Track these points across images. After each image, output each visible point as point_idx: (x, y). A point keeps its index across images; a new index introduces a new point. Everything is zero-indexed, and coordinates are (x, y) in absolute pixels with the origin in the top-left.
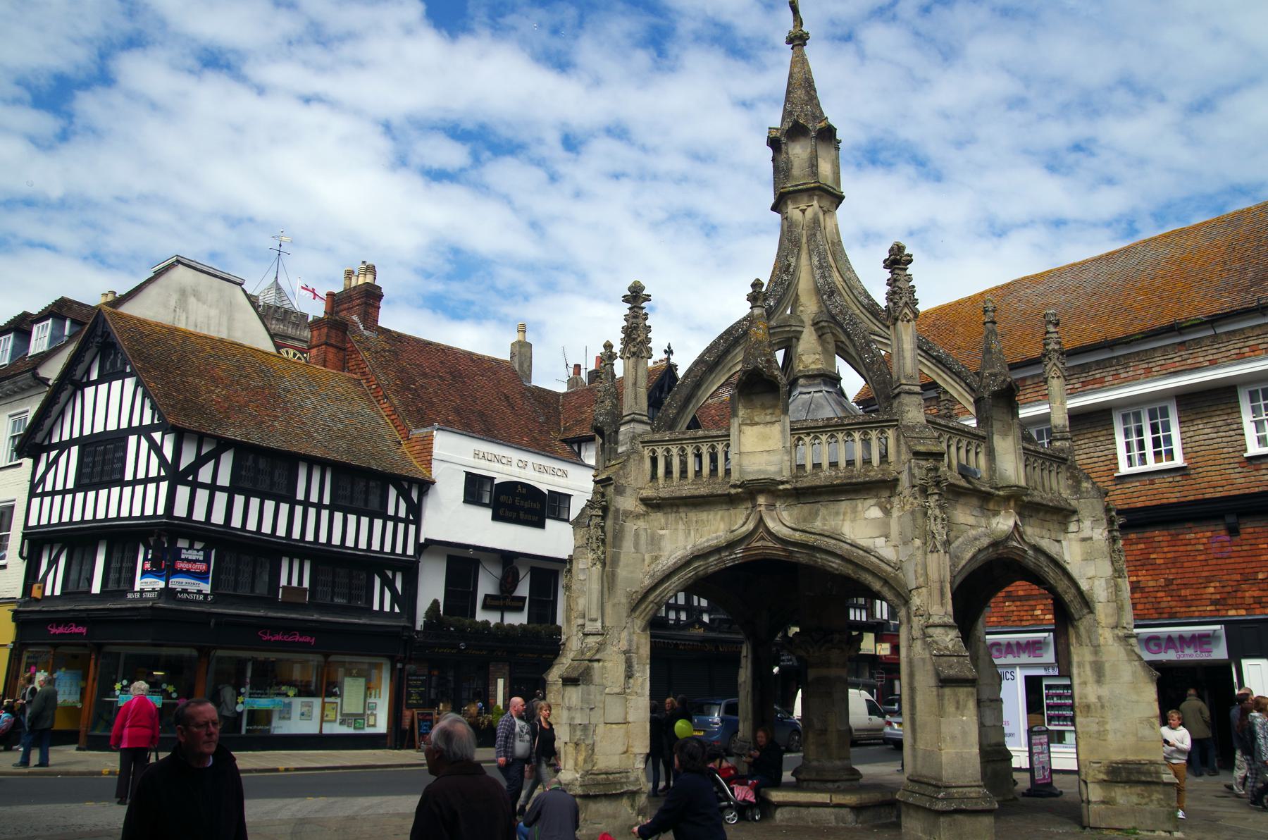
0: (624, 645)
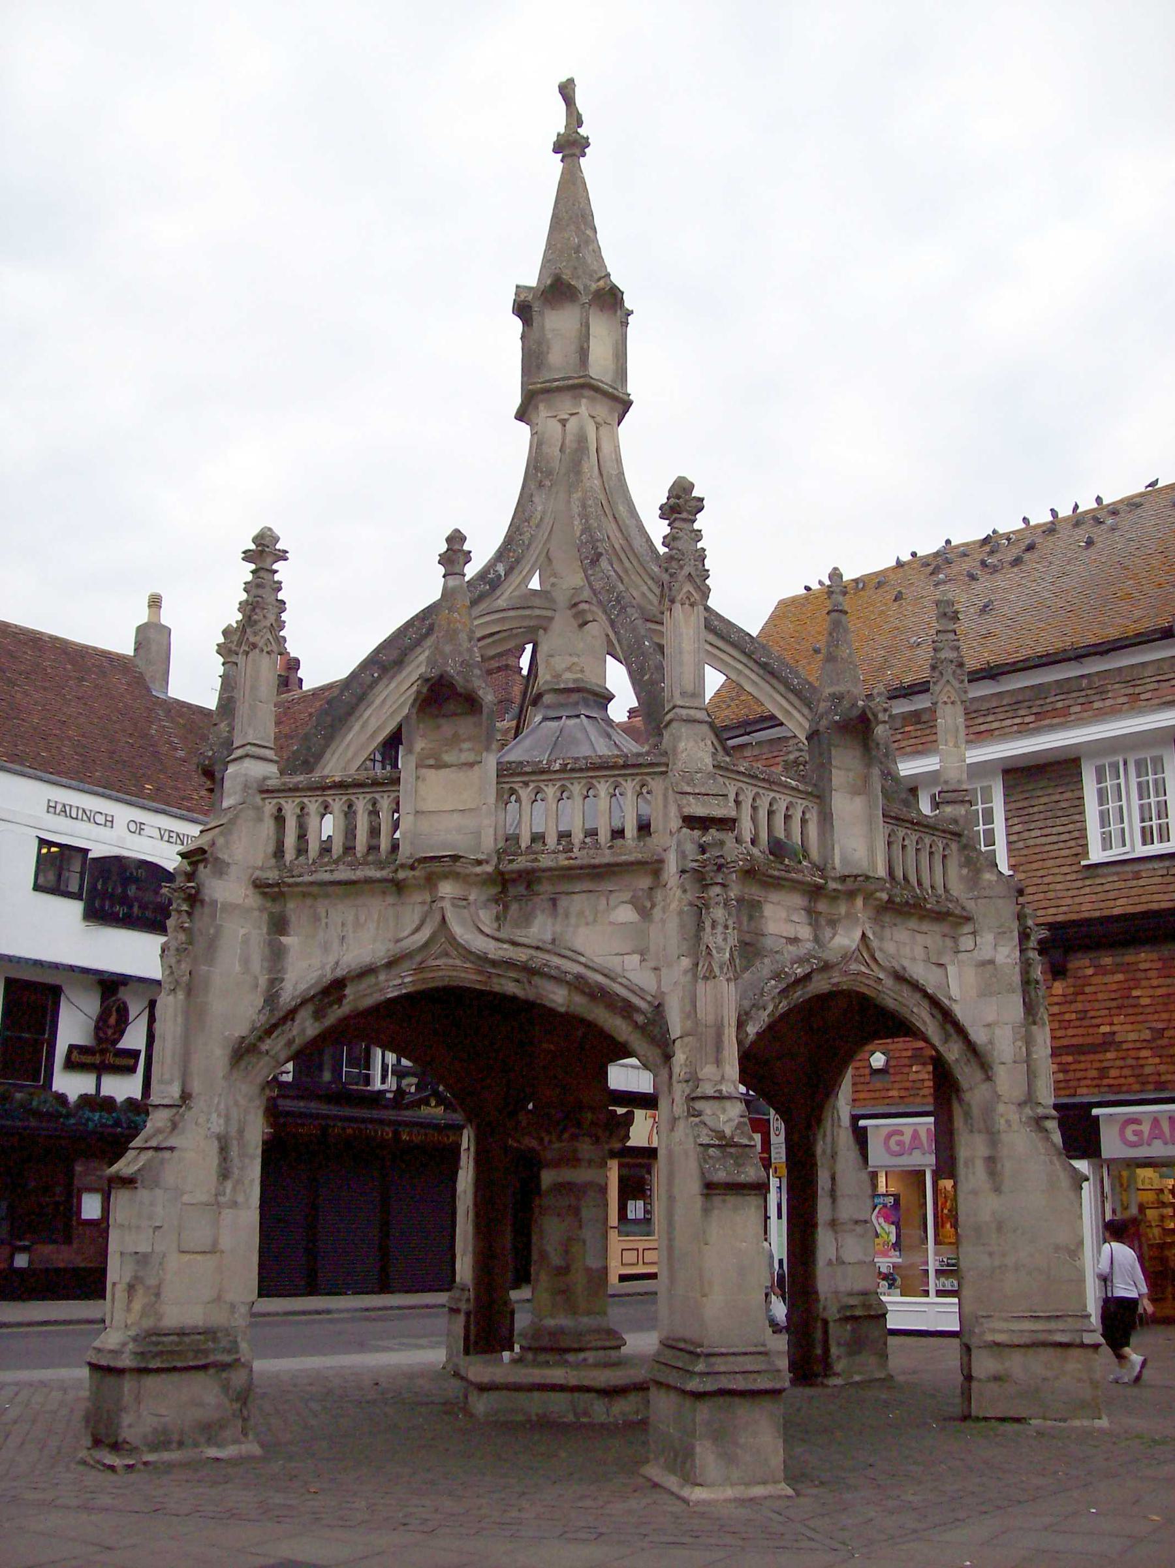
0: (217, 1125)
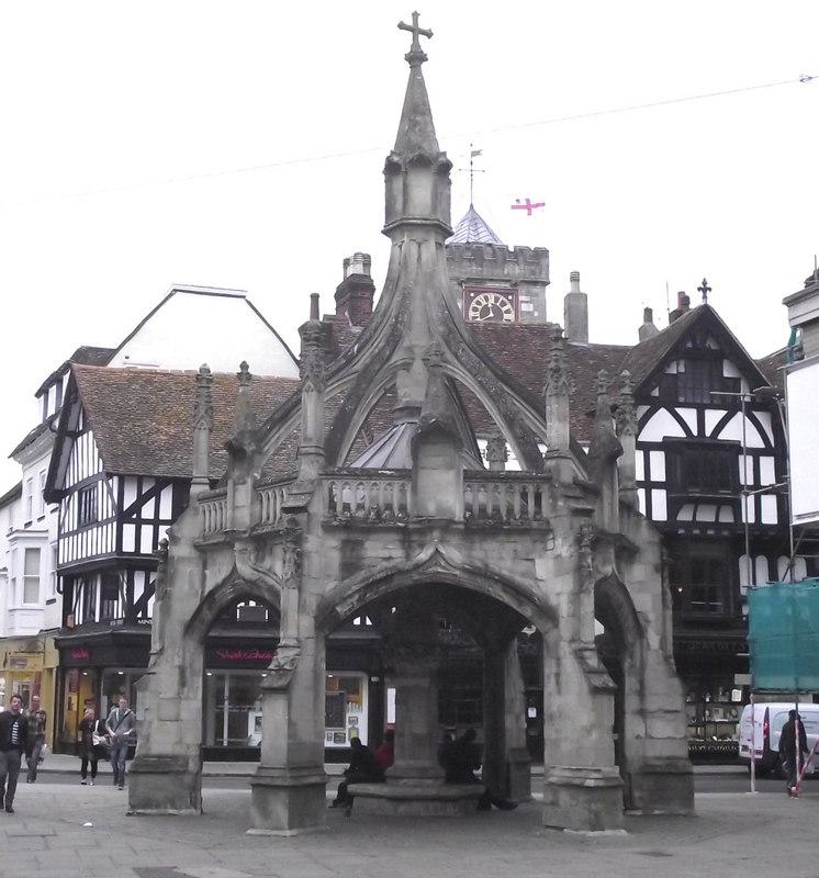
0: (177, 661)
